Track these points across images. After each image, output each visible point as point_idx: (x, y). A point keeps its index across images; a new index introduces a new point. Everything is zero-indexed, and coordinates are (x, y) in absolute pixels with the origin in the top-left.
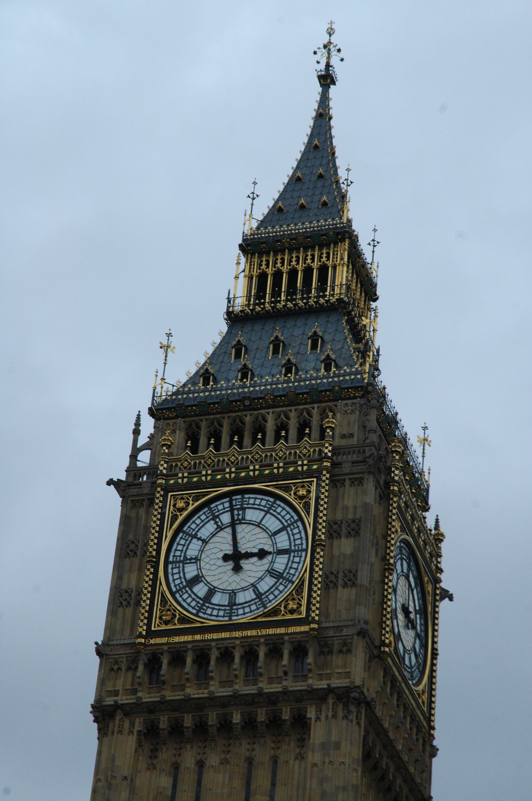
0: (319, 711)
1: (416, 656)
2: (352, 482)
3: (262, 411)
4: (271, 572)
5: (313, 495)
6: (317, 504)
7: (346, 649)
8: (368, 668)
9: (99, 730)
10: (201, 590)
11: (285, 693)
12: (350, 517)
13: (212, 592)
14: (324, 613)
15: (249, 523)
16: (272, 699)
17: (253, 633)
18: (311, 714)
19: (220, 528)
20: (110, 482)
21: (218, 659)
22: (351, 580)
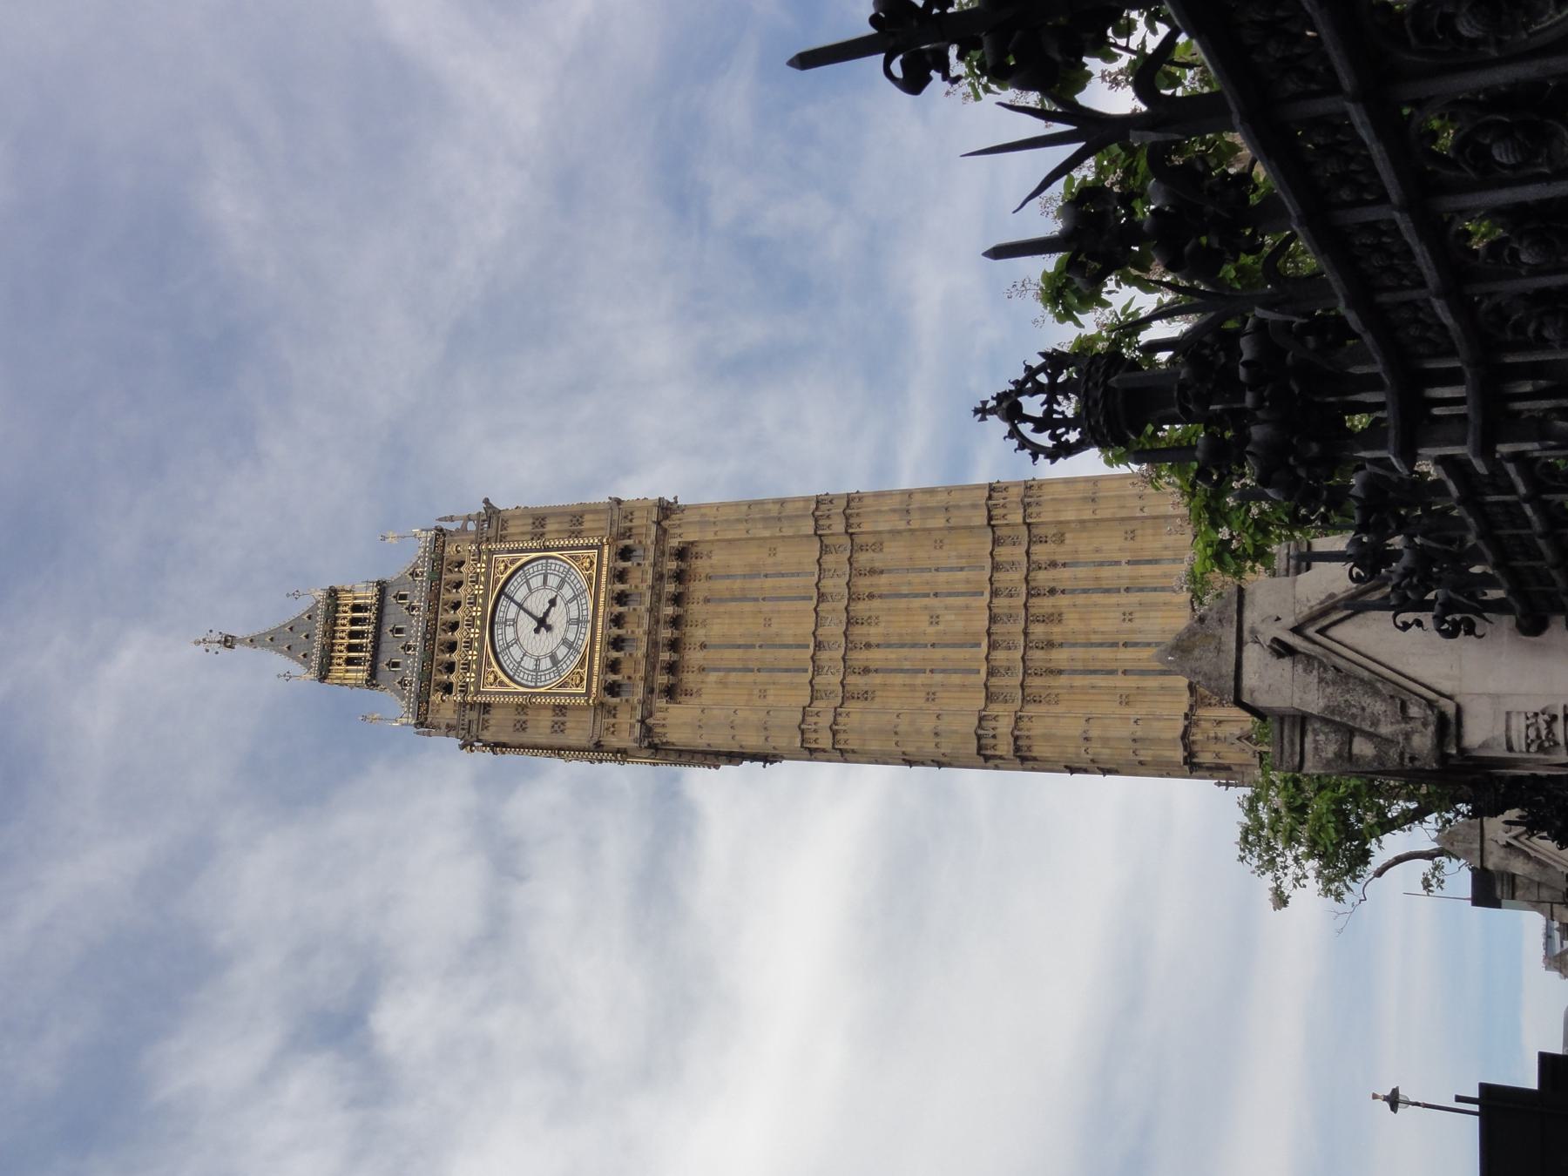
10: (562, 652)
13: (565, 641)
16: (659, 577)
17: (602, 595)
18: (674, 543)
19: (517, 640)
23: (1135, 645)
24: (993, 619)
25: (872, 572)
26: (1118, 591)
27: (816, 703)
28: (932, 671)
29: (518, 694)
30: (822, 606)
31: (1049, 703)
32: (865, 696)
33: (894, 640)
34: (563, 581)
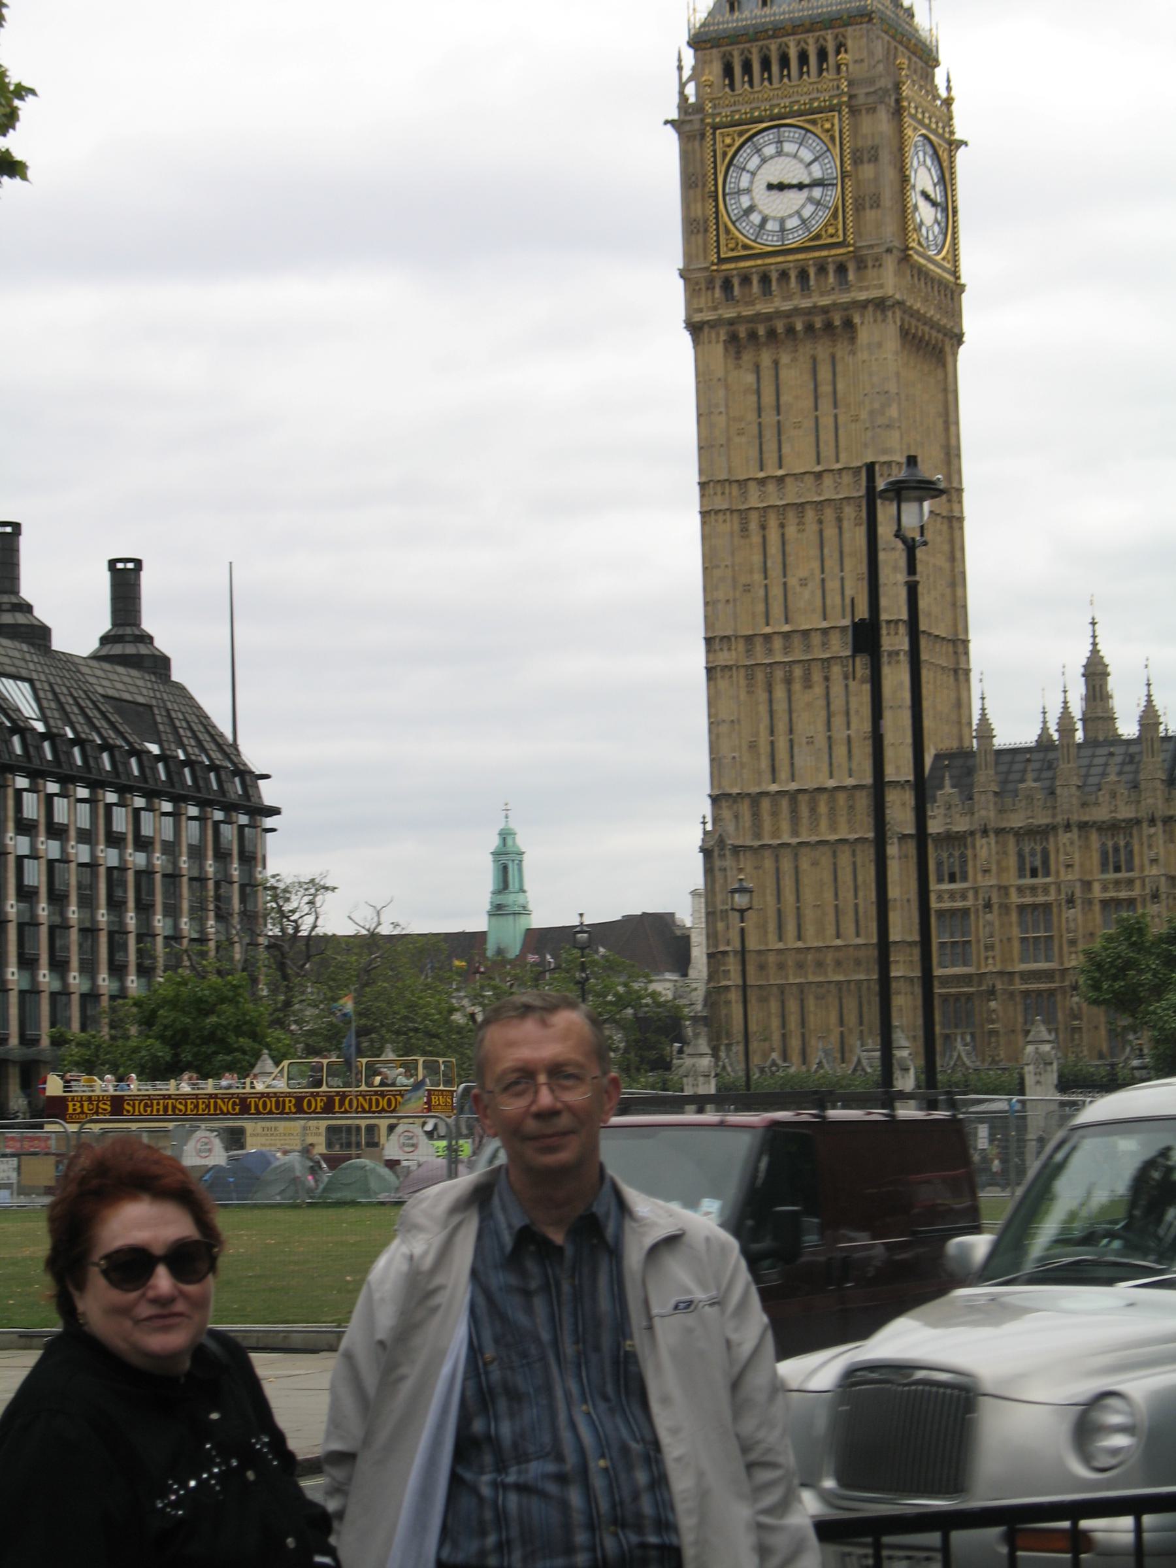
0: (862, 316)
1: (939, 224)
2: (868, 110)
3: (785, 39)
4: (810, 199)
5: (837, 128)
6: (841, 137)
7: (878, 263)
8: (899, 273)
9: (694, 341)
10: (755, 218)
11: (834, 304)
12: (870, 143)
13: (764, 220)
14: (858, 234)
15: (787, 155)
16: (825, 310)
18: (857, 320)
19: (764, 161)
20: (666, 122)
21: (779, 280)
22: (876, 204)
23: (792, 747)
24: (806, 633)
25: (839, 520)
26: (829, 730)
27: (735, 486)
28: (766, 586)
29: (716, 180)
30: (812, 477)
31: (747, 686)
32: (744, 529)
33: (788, 549)
34: (818, 203)
